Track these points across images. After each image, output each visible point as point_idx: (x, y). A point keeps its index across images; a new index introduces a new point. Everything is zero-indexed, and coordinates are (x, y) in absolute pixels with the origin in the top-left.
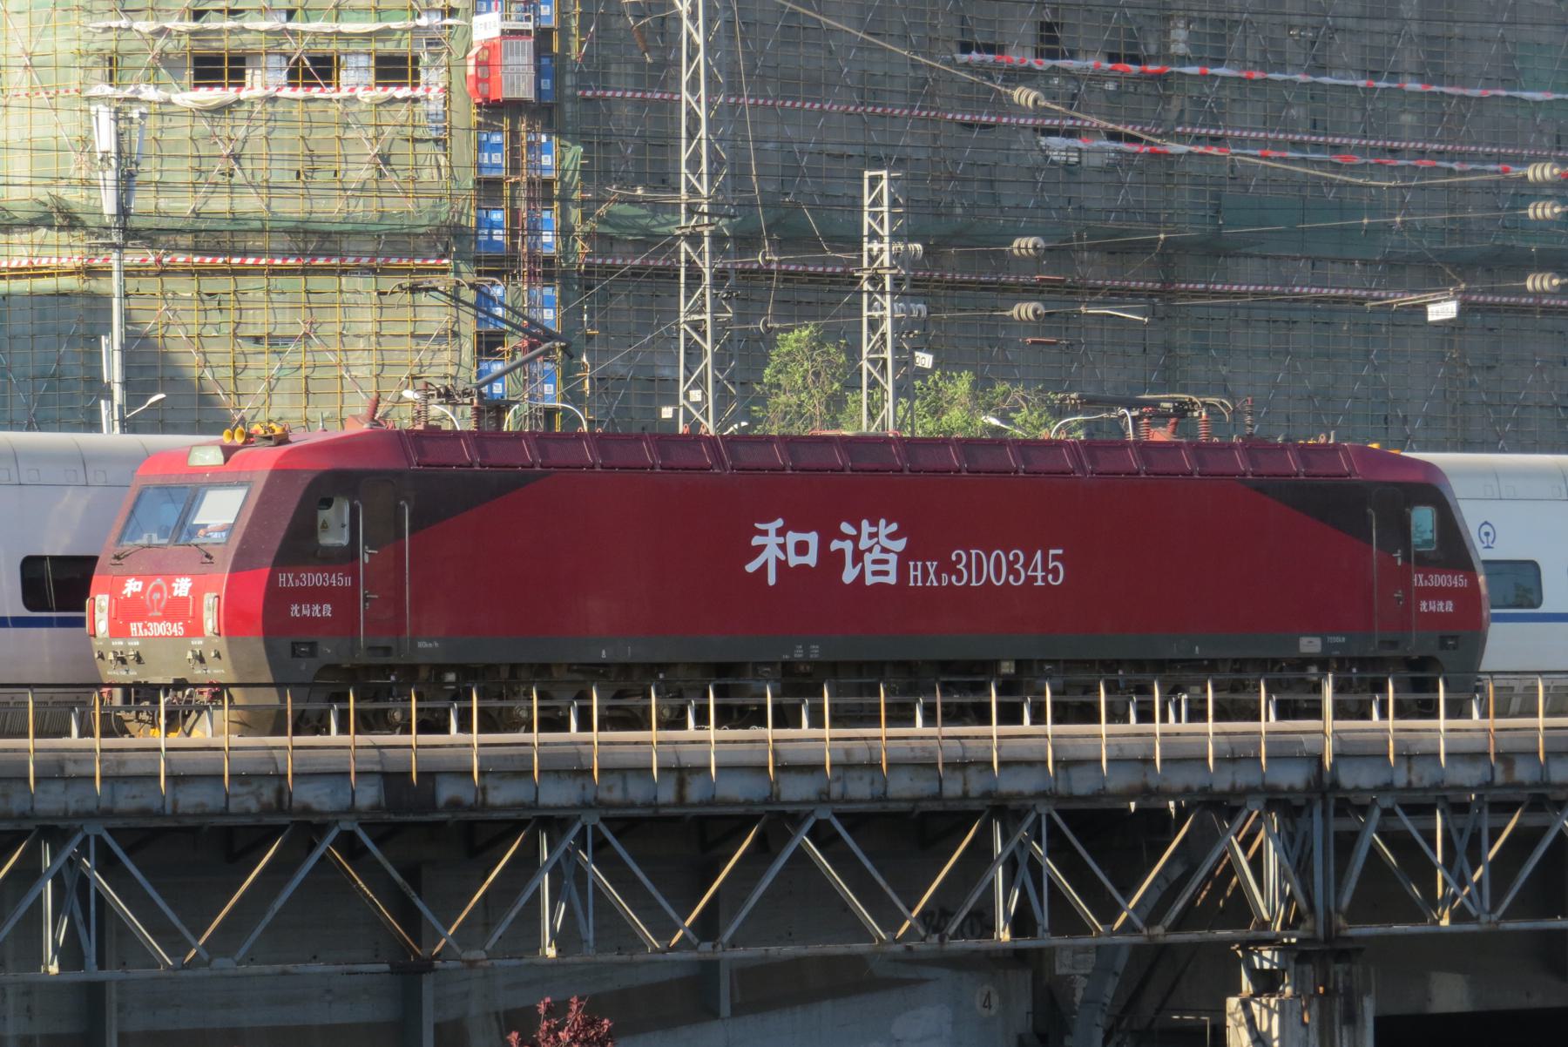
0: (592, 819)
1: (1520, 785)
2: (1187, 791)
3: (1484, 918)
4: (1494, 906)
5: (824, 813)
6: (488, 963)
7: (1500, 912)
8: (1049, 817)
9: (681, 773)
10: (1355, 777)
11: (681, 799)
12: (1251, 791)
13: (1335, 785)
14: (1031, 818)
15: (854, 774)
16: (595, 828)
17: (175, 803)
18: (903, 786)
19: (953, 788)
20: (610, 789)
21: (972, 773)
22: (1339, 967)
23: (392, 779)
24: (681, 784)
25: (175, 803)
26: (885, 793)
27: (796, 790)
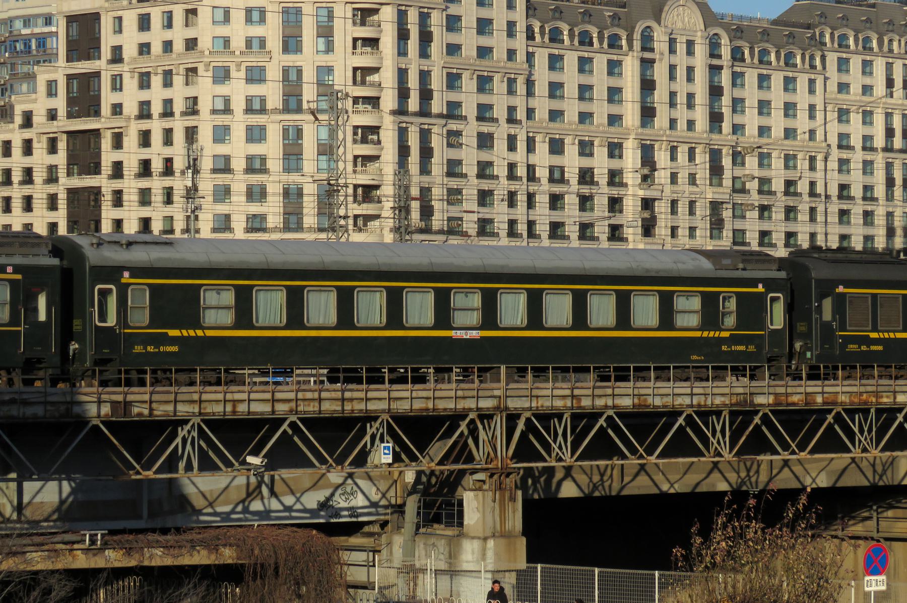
0: (197, 420)
1: (584, 408)
2: (445, 409)
3: (568, 460)
4: (572, 456)
5: (293, 418)
6: (153, 476)
7: (575, 458)
8: (387, 421)
9: (234, 401)
10: (513, 404)
11: (234, 412)
12: (470, 410)
13: (507, 408)
14: (380, 420)
15: (306, 403)
16: (199, 425)
17: (24, 413)
18: (327, 406)
19: (348, 407)
20: (205, 409)
21: (355, 402)
22: (508, 480)
23: (114, 403)
24: (234, 407)
25: (24, 413)
26: (320, 411)
27: (281, 408)
